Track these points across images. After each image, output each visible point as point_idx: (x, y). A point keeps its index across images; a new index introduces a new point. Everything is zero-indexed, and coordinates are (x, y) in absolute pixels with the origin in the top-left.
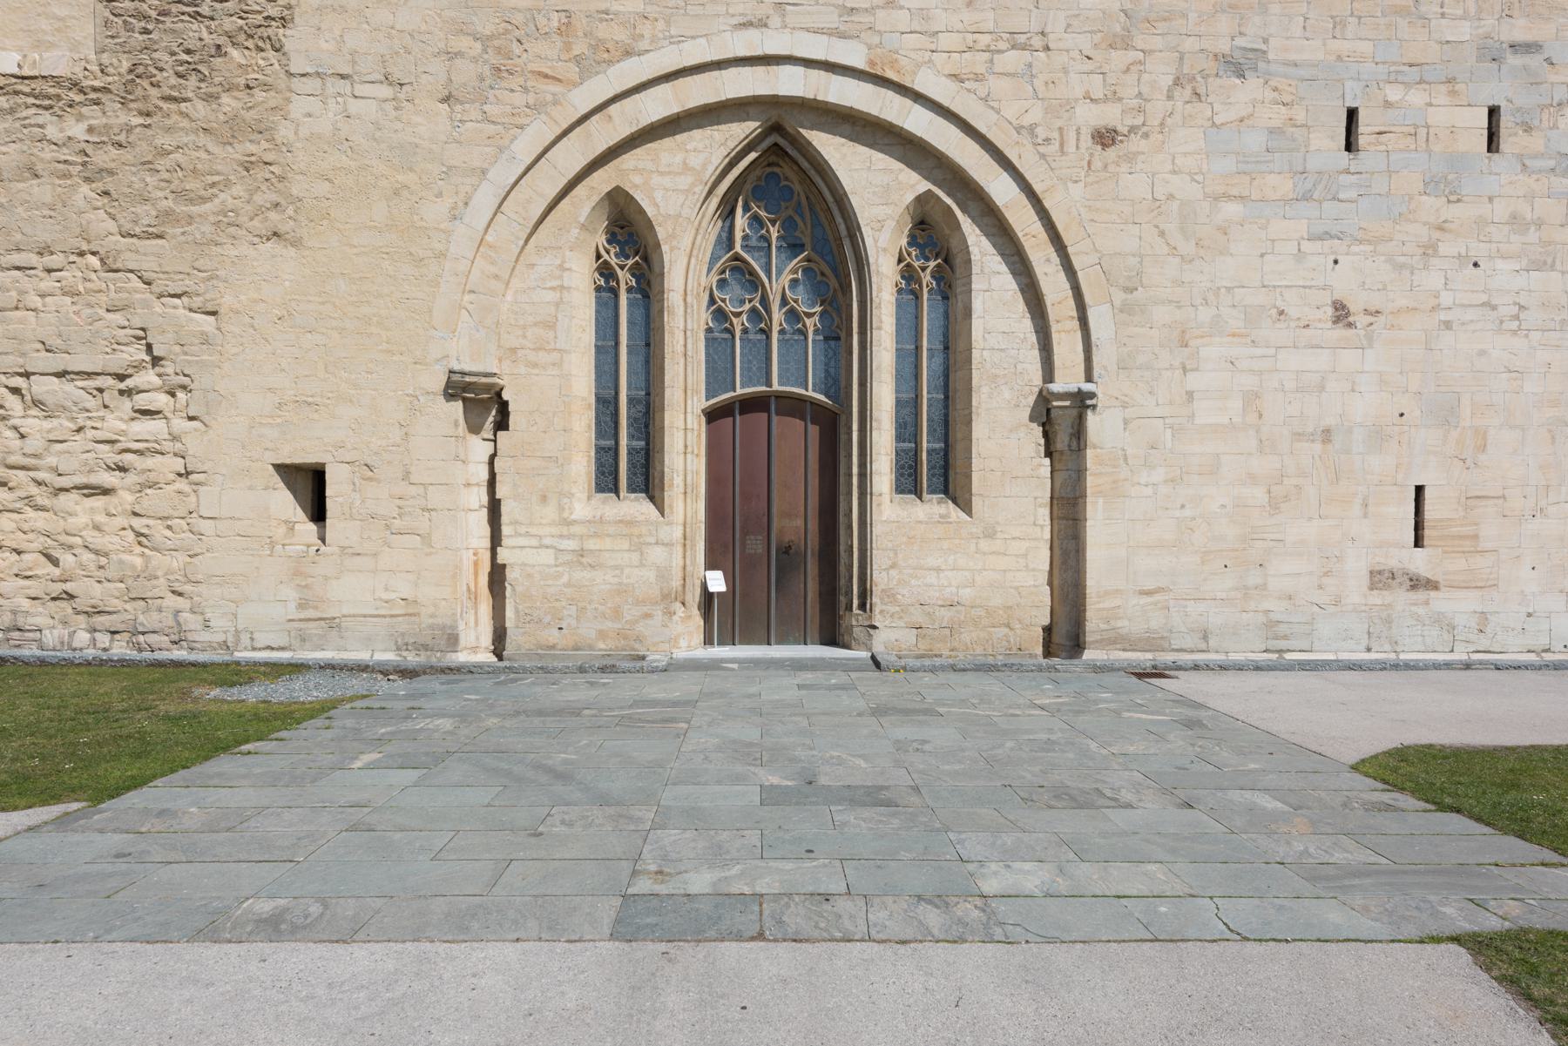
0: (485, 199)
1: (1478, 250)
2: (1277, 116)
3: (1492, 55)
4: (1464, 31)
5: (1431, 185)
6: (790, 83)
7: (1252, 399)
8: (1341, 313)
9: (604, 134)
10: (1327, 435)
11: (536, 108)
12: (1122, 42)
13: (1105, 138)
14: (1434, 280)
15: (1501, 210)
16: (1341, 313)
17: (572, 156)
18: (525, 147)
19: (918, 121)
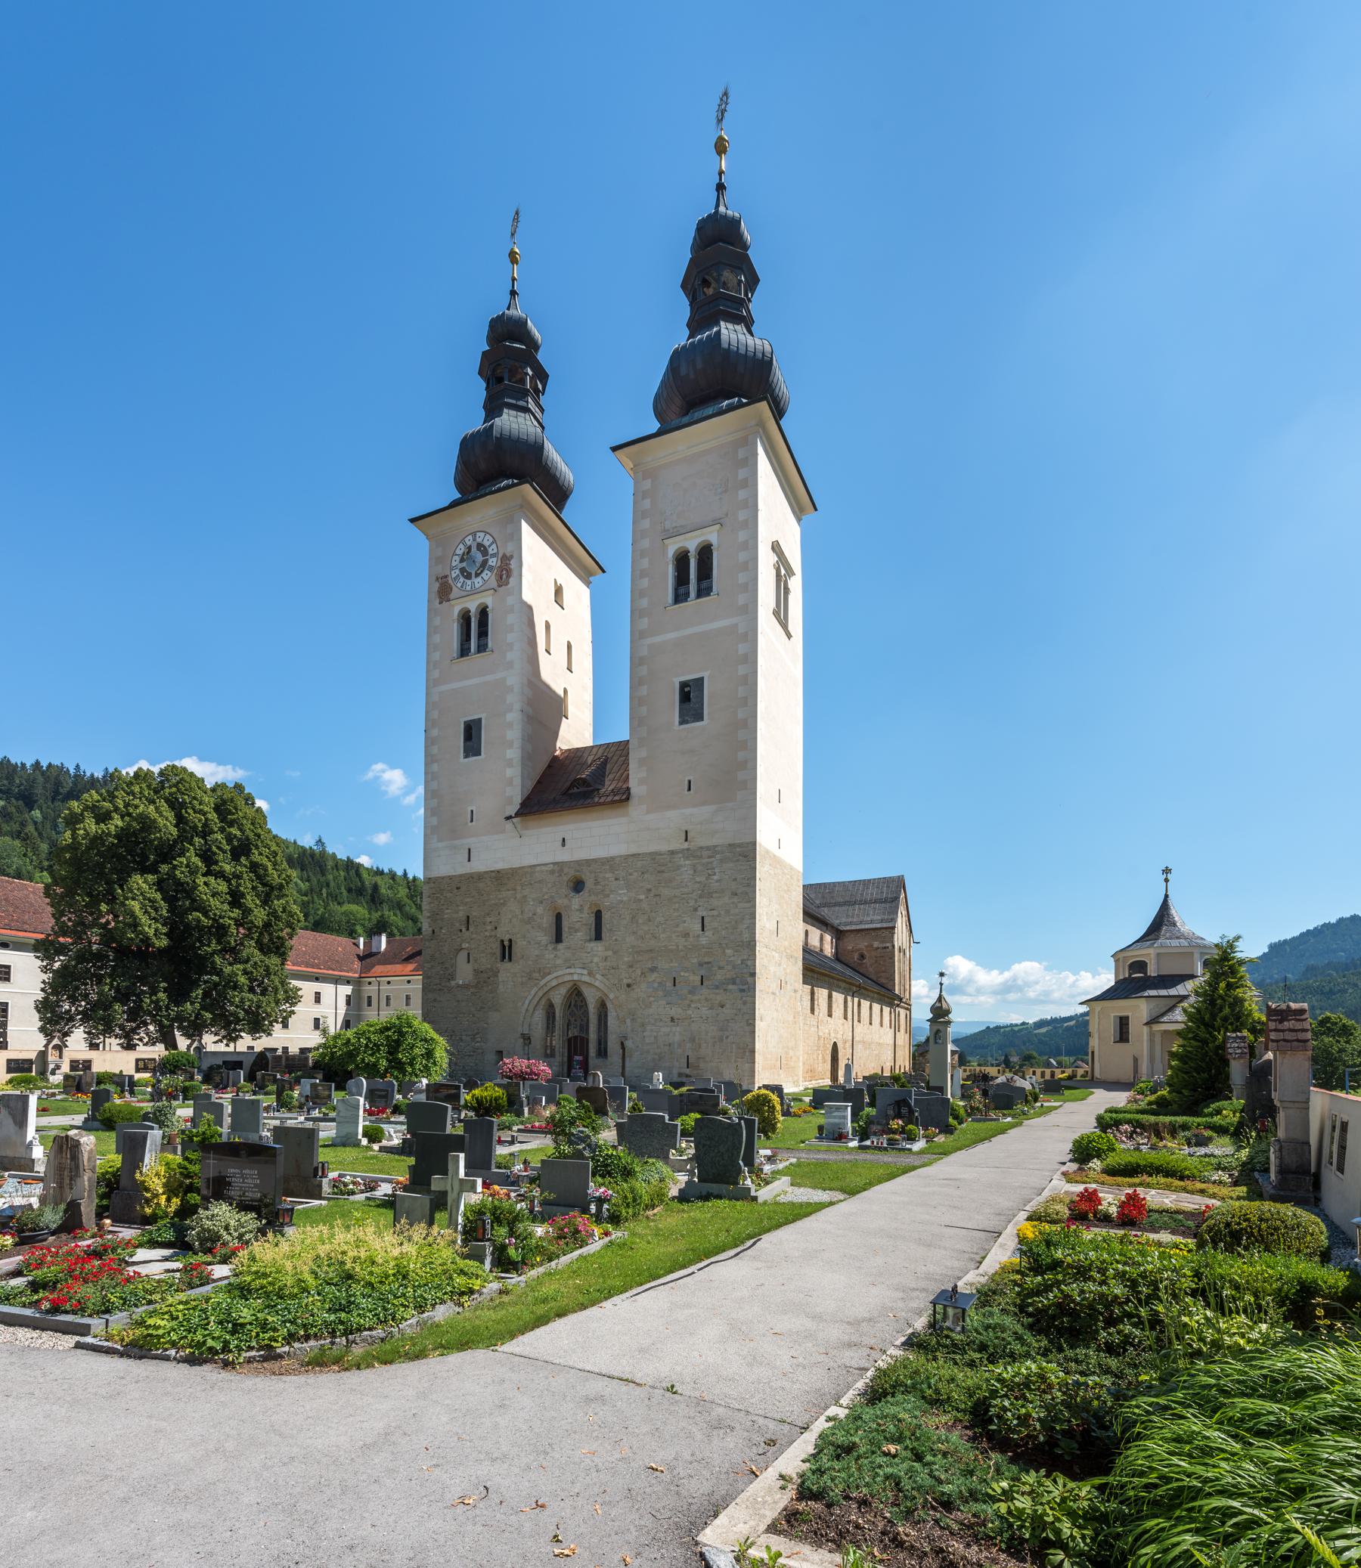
0: (527, 1002)
1: (699, 1005)
2: (659, 980)
3: (701, 965)
4: (695, 961)
5: (690, 992)
6: (576, 978)
7: (655, 1037)
8: (672, 1020)
9: (546, 989)
10: (670, 1045)
11: (536, 985)
12: (631, 967)
13: (629, 986)
14: (690, 1012)
15: (703, 997)
16: (672, 1020)
17: (541, 994)
18: (533, 992)
19: (597, 984)
